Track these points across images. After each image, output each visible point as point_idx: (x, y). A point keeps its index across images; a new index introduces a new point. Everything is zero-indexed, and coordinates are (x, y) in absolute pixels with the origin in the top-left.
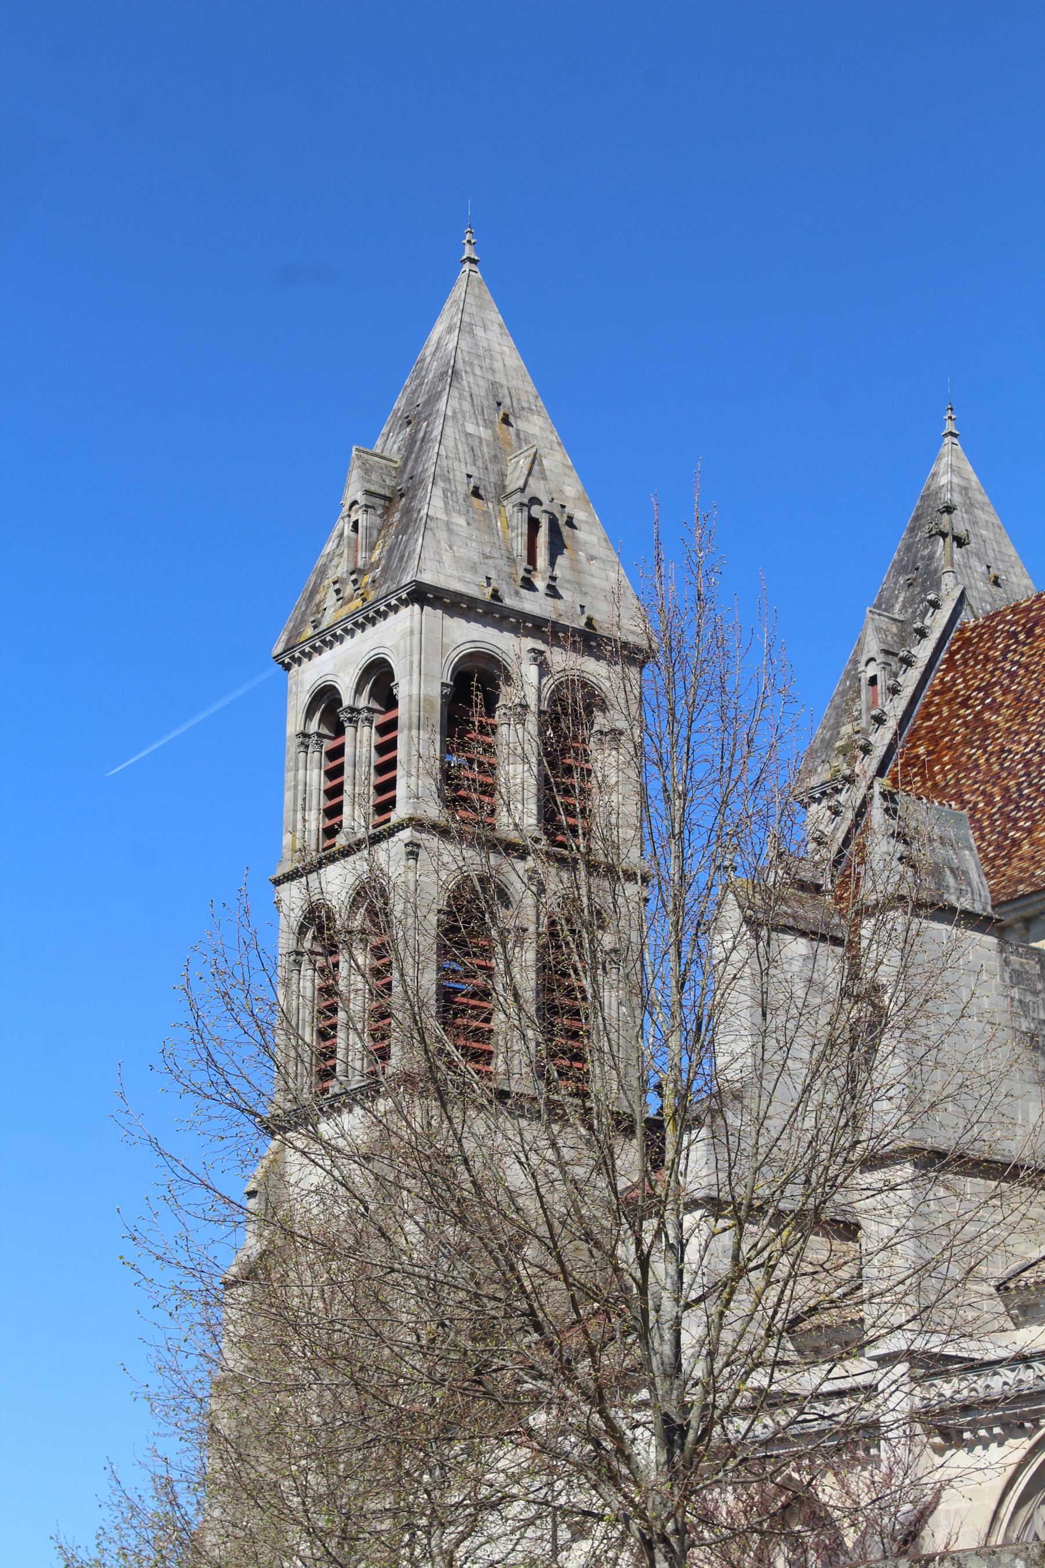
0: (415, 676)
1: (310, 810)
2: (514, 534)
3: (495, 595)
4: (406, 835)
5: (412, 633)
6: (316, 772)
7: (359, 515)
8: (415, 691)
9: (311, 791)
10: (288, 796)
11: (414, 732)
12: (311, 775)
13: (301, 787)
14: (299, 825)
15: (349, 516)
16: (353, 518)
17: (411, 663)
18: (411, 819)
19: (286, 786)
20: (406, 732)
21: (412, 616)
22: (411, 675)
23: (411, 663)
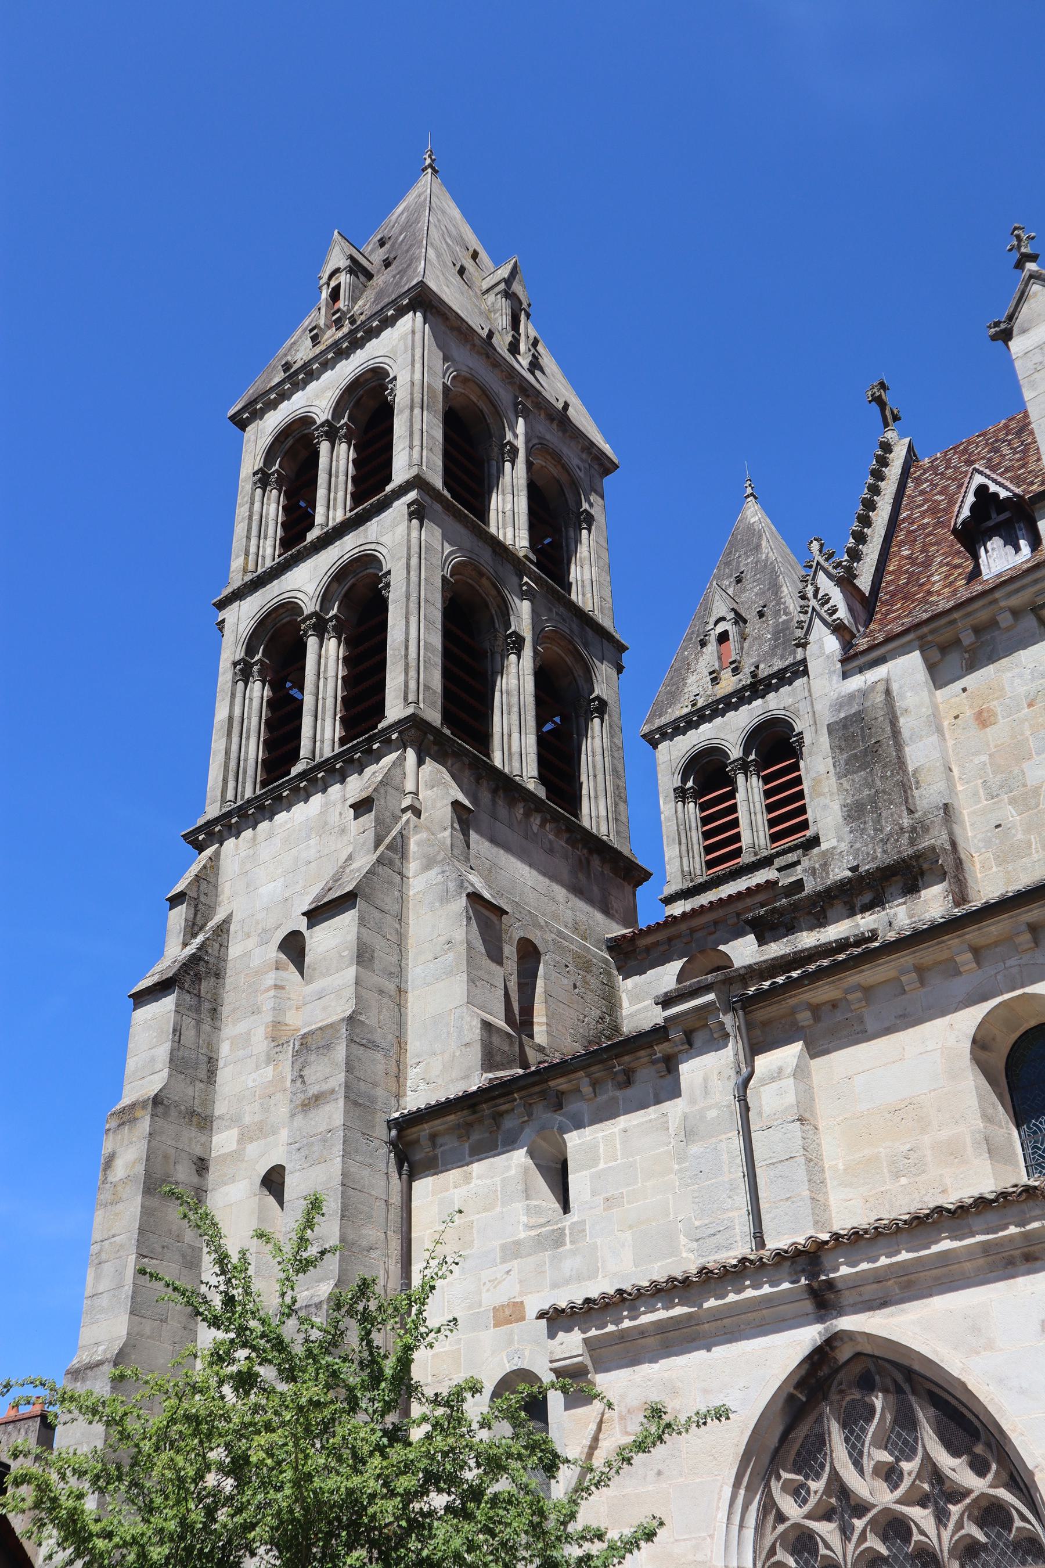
0: (418, 366)
1: (265, 538)
2: (498, 315)
3: (491, 334)
4: (412, 495)
5: (413, 332)
6: (273, 506)
7: (344, 279)
8: (418, 376)
9: (267, 522)
10: (240, 529)
11: (417, 411)
12: (268, 510)
13: (256, 517)
14: (253, 550)
15: (328, 285)
16: (333, 284)
17: (413, 356)
18: (417, 477)
19: (238, 519)
20: (407, 412)
21: (414, 320)
22: (413, 365)
23: (413, 356)
